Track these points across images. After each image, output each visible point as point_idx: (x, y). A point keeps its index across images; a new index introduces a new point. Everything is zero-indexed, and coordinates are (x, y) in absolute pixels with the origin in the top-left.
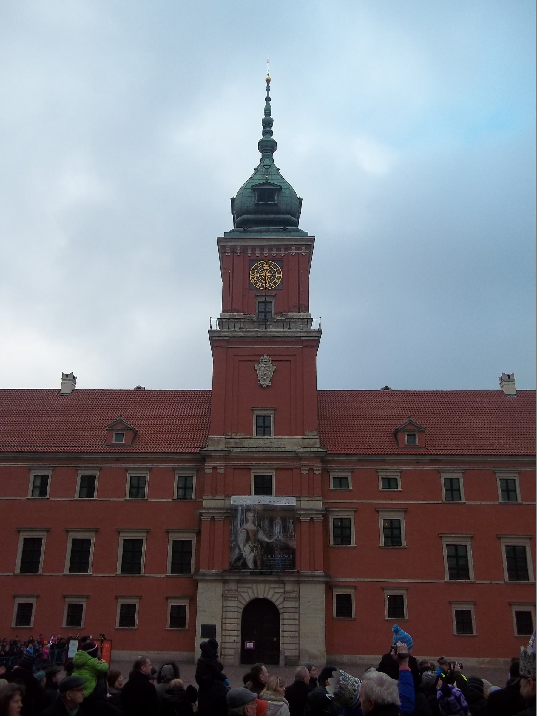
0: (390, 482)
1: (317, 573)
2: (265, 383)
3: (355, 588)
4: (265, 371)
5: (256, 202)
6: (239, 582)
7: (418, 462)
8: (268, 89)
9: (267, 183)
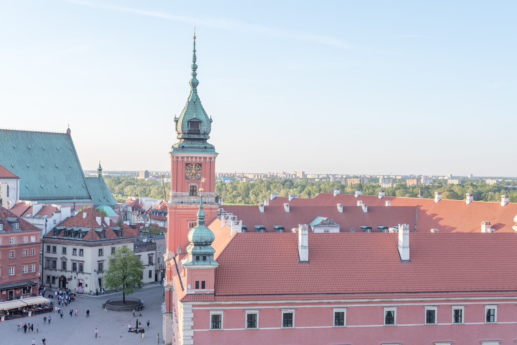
8: (195, 45)
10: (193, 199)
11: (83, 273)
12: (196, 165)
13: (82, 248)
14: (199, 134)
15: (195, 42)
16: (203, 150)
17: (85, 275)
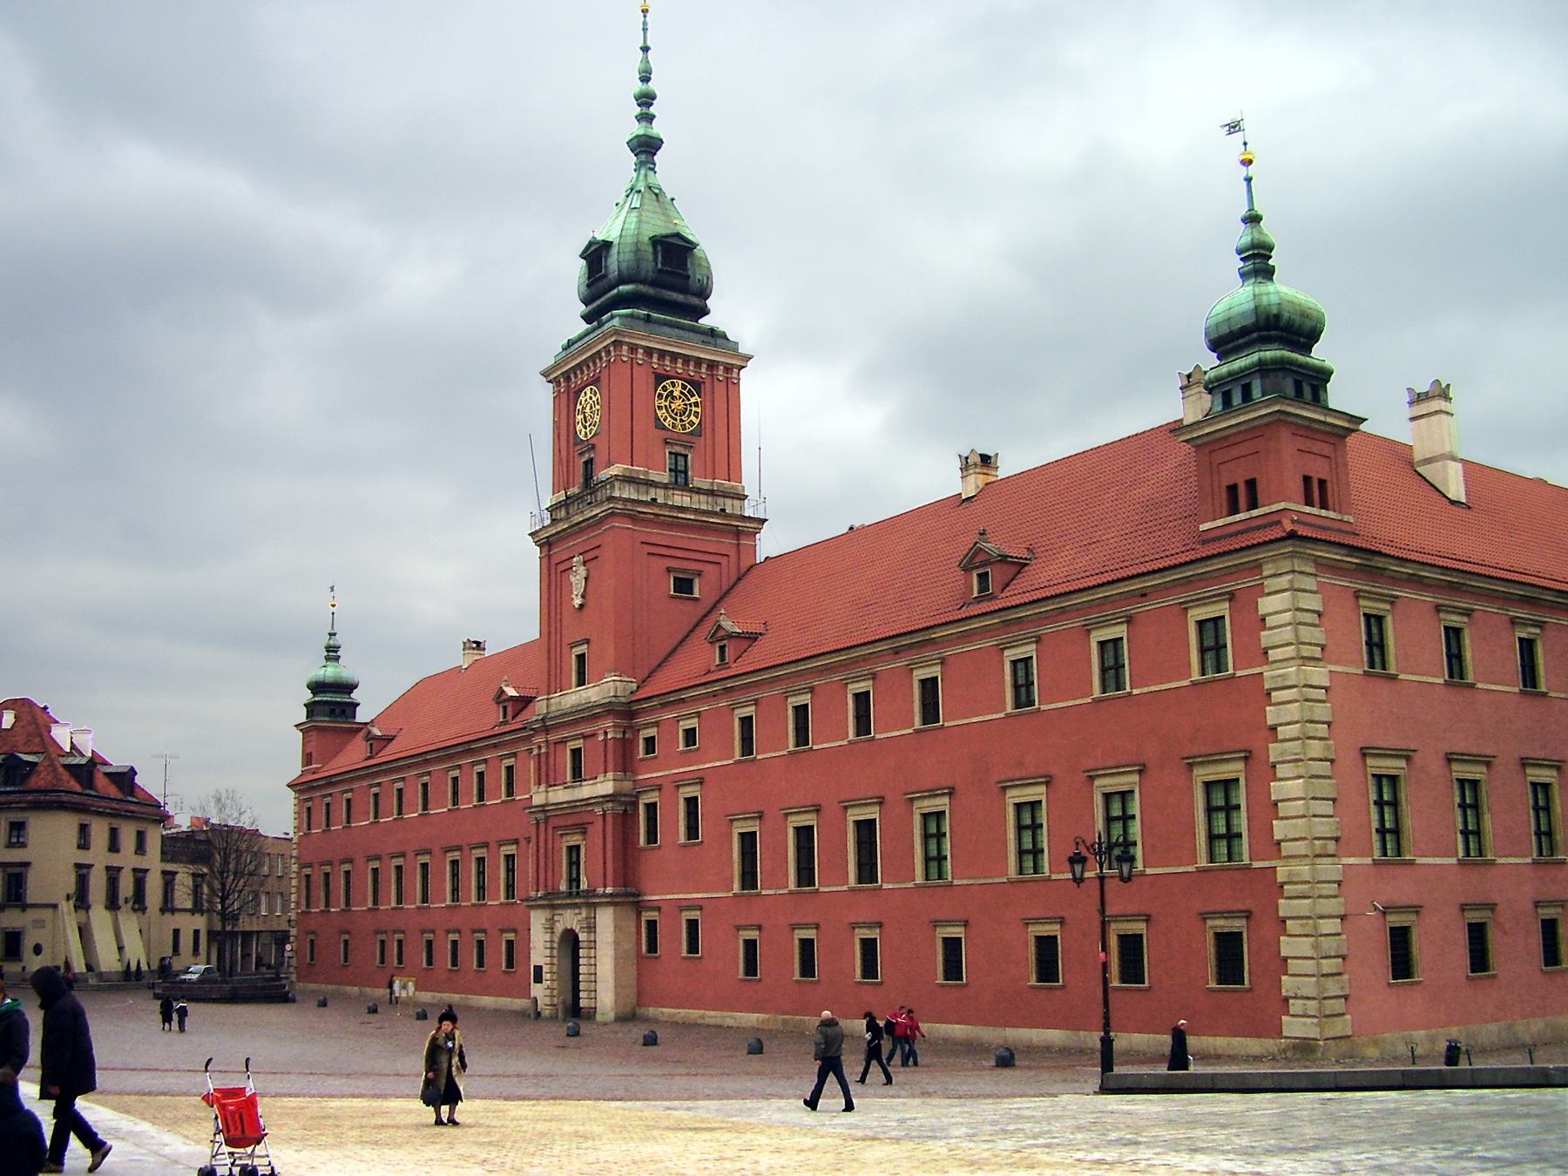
0: (690, 735)
1: (609, 890)
2: (577, 602)
3: (659, 909)
4: (577, 579)
5: (584, 280)
6: (553, 907)
7: (714, 695)
8: (645, 30)
9: (590, 244)
10: (681, 499)
11: (25, 907)
12: (684, 387)
13: (18, 817)
14: (684, 290)
15: (645, 23)
16: (705, 338)
17: (32, 915)
